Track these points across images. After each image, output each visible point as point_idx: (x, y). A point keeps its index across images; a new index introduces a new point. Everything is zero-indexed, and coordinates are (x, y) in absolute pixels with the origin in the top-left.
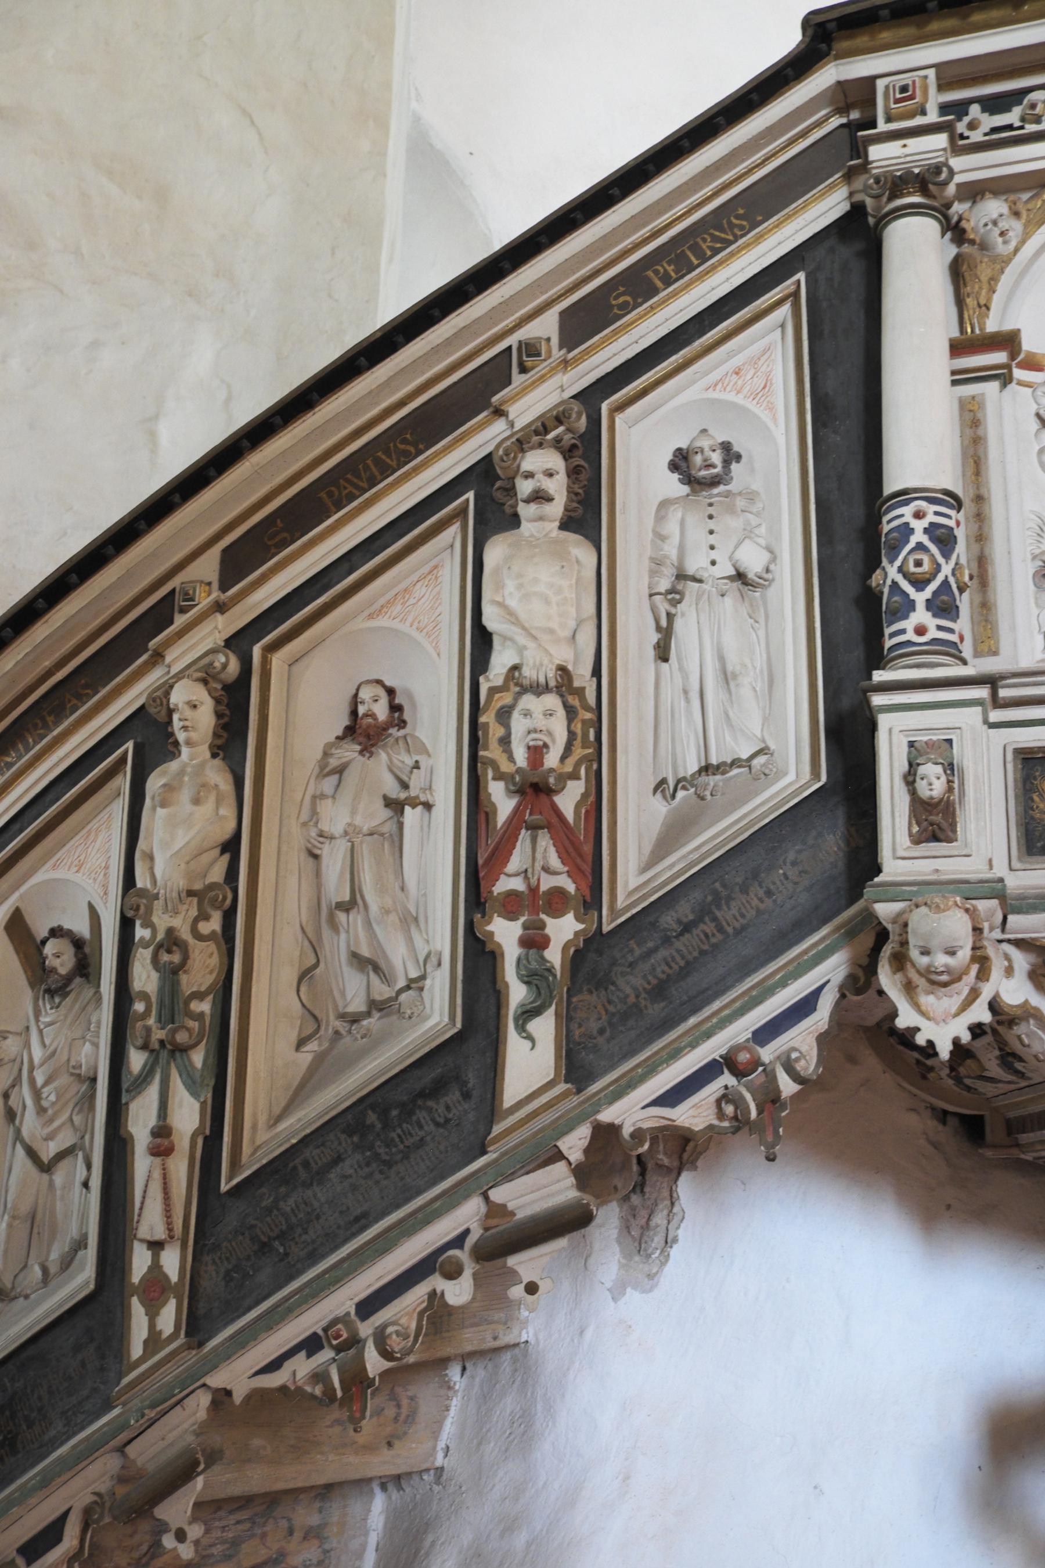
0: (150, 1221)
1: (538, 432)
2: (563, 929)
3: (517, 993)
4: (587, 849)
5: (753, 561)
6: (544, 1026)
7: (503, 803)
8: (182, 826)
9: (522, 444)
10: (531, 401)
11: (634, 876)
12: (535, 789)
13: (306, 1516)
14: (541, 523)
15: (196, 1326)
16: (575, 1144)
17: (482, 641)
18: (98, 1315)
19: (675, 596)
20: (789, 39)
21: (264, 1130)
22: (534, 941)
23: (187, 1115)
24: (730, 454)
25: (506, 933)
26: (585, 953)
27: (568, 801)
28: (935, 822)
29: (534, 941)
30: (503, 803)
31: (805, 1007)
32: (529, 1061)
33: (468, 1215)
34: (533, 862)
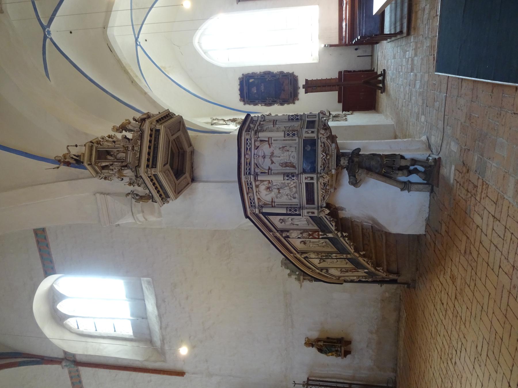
0: (342, 257)
1: (281, 235)
2: (320, 233)
3: (325, 236)
4: (315, 231)
5: (290, 219)
6: (328, 234)
7: (311, 237)
8: (313, 256)
9: (282, 236)
10: (278, 235)
11: (316, 228)
12: (310, 235)
13: (365, 231)
14: (288, 234)
15: (349, 254)
16: (336, 232)
17: (299, 238)
18: (348, 259)
19: (293, 224)
20: (248, 219)
21: (335, 250)
22: (321, 235)
23: (334, 255)
24: (280, 219)
25: (321, 237)
26: (322, 231)
27: (311, 233)
28: (313, 213)
29: (321, 235)
30: (311, 237)
31: (326, 217)
32: (330, 235)
33: (341, 239)
34: (316, 235)
